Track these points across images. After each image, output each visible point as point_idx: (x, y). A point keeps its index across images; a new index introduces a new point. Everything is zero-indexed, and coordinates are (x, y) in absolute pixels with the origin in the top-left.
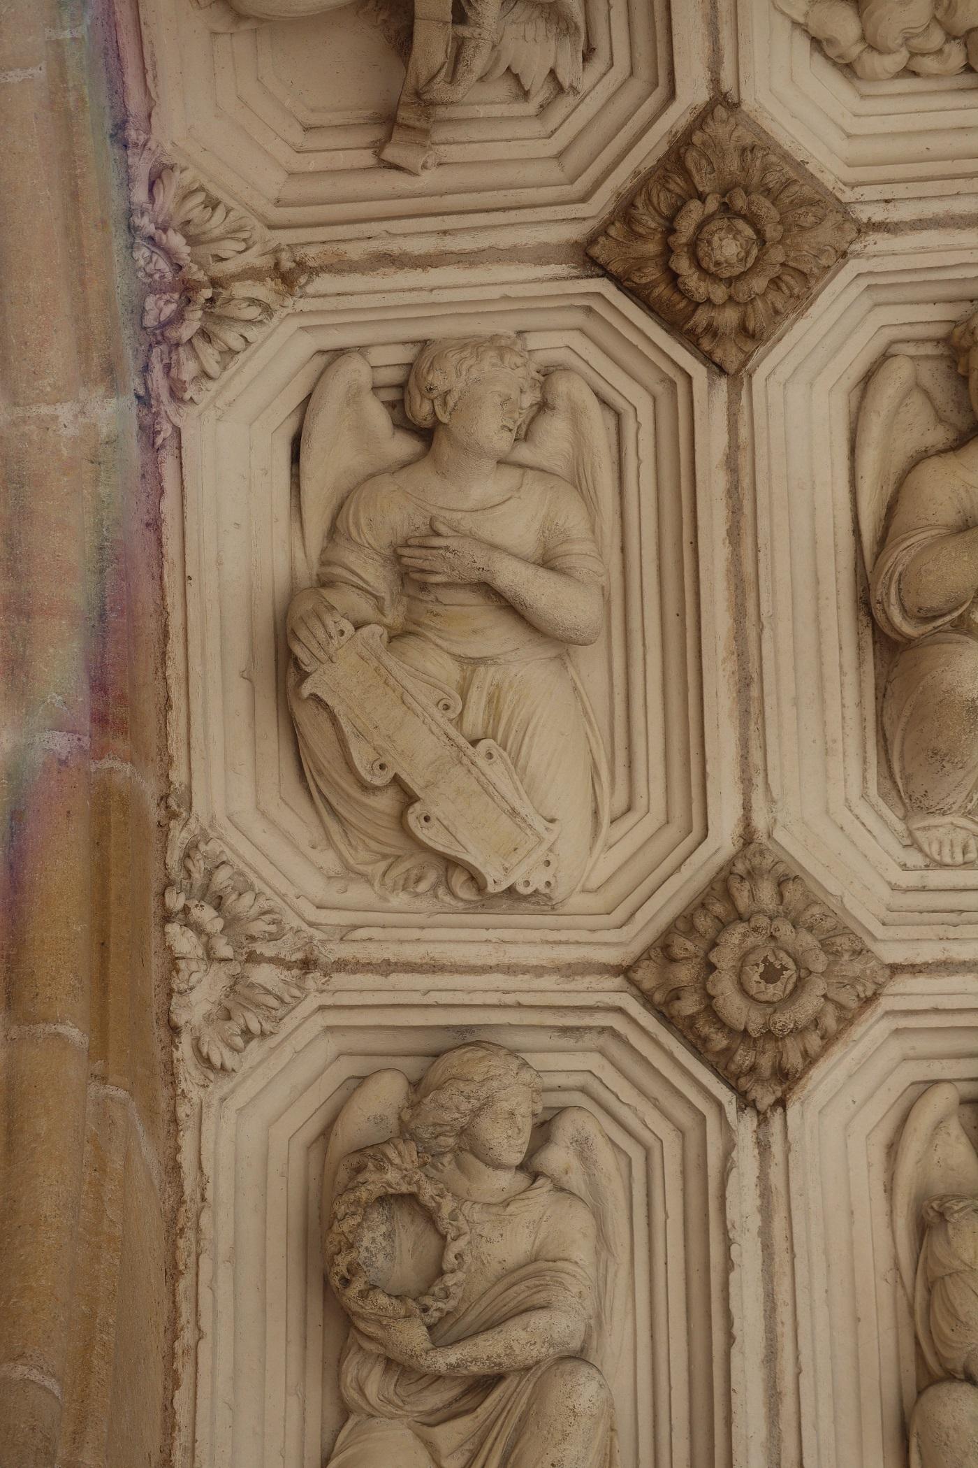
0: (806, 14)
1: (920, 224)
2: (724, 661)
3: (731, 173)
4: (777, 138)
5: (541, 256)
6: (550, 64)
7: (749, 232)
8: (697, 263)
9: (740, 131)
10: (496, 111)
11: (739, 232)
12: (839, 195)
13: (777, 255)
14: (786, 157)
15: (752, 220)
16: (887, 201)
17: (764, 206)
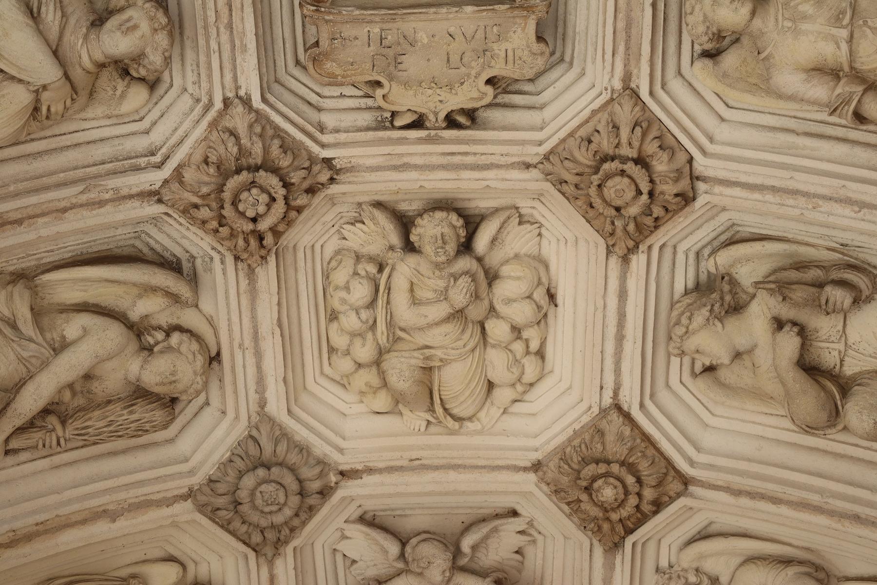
0: (499, 408)
1: (618, 371)
2: (844, 526)
3: (569, 482)
4: (559, 443)
5: (610, 567)
6: (514, 534)
7: (600, 482)
8: (625, 486)
9: (551, 465)
10: (540, 555)
11: (600, 487)
12: (594, 415)
13: (615, 468)
14: (570, 440)
15: (594, 479)
16: (602, 388)
17: (590, 470)
